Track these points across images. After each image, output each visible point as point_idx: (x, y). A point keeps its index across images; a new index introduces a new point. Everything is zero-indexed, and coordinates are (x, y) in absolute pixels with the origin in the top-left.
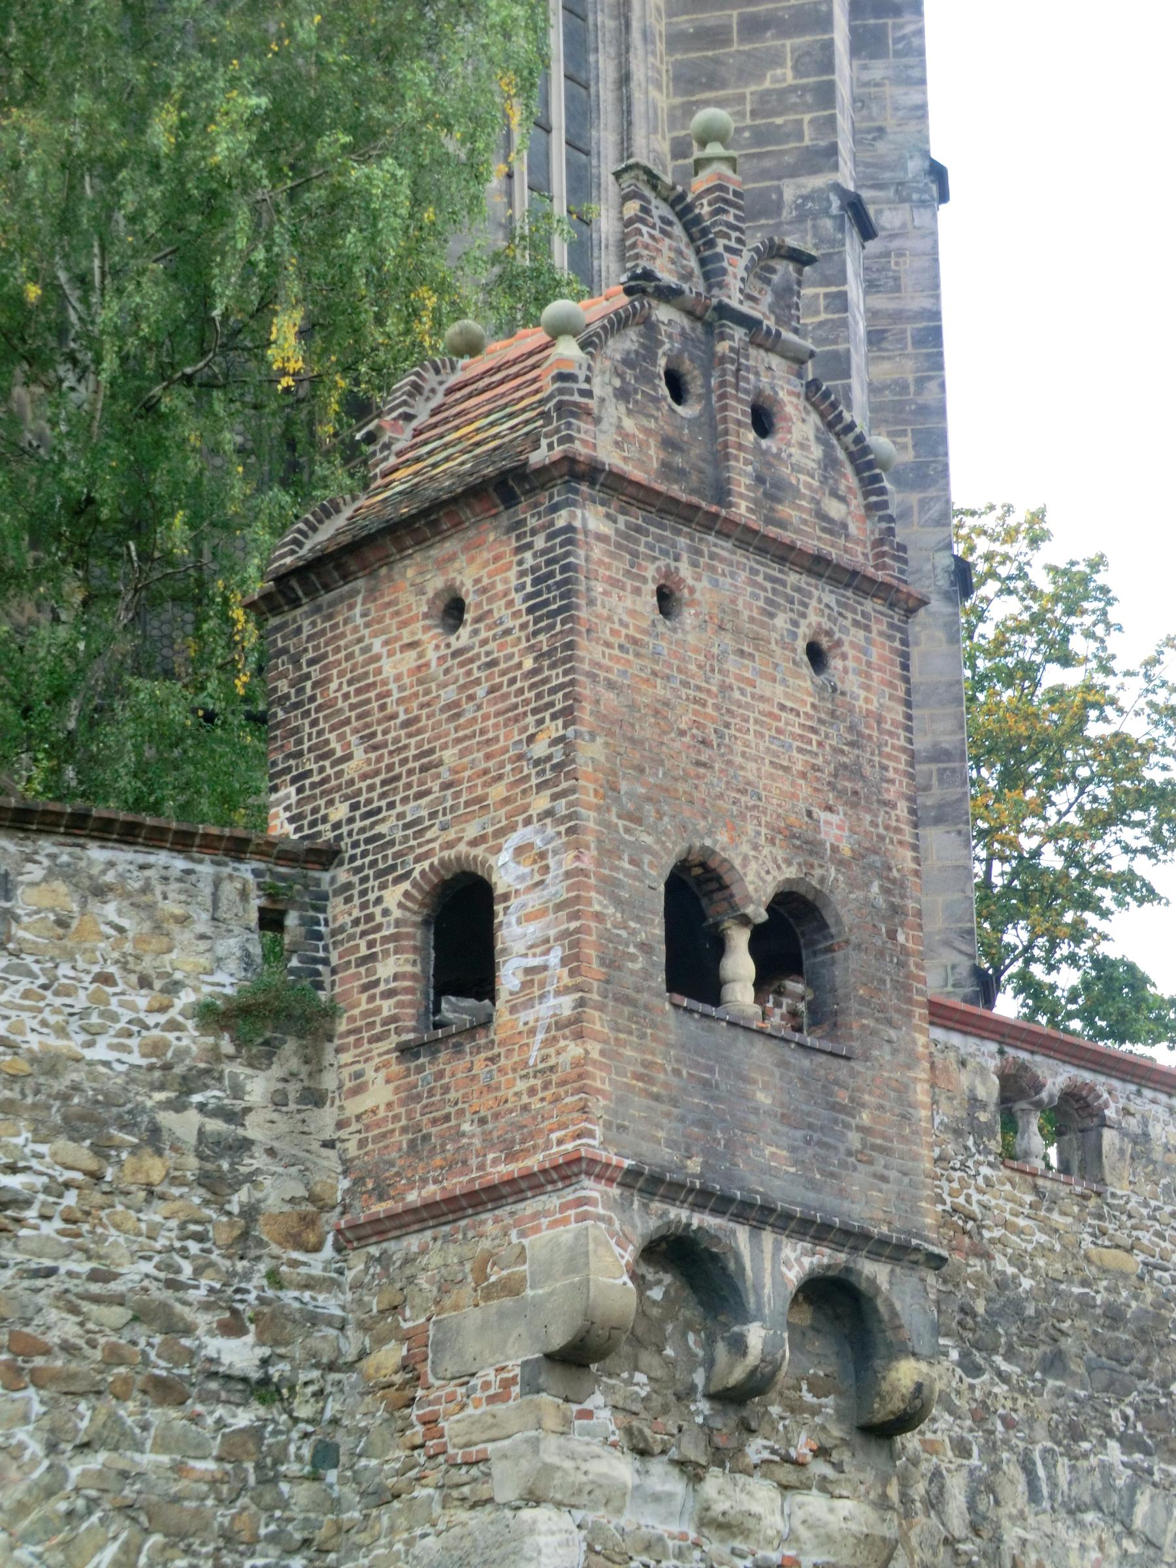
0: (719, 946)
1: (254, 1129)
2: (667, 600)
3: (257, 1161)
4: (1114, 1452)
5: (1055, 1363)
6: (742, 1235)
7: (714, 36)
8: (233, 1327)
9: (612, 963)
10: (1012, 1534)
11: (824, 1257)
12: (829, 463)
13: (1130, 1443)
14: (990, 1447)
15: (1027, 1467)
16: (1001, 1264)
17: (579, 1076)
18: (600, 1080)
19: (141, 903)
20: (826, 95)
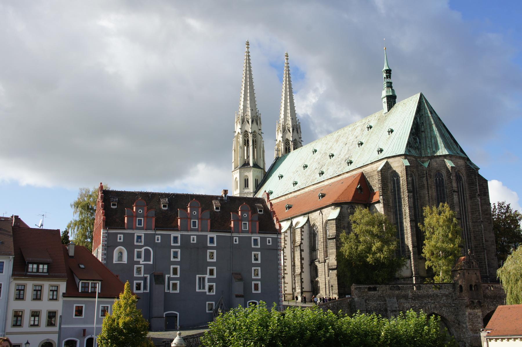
0: (472, 287)
1: (453, 295)
2: (469, 273)
3: (454, 297)
4: (495, 302)
5: (491, 299)
6: (474, 300)
7: (473, 212)
8: (453, 304)
9: (467, 290)
10: (489, 307)
11: (478, 300)
12: (476, 264)
13: (496, 302)
14: (488, 303)
15: (490, 304)
16: (488, 295)
17: (466, 295)
18: (467, 295)
19: (448, 287)
20: (480, 215)
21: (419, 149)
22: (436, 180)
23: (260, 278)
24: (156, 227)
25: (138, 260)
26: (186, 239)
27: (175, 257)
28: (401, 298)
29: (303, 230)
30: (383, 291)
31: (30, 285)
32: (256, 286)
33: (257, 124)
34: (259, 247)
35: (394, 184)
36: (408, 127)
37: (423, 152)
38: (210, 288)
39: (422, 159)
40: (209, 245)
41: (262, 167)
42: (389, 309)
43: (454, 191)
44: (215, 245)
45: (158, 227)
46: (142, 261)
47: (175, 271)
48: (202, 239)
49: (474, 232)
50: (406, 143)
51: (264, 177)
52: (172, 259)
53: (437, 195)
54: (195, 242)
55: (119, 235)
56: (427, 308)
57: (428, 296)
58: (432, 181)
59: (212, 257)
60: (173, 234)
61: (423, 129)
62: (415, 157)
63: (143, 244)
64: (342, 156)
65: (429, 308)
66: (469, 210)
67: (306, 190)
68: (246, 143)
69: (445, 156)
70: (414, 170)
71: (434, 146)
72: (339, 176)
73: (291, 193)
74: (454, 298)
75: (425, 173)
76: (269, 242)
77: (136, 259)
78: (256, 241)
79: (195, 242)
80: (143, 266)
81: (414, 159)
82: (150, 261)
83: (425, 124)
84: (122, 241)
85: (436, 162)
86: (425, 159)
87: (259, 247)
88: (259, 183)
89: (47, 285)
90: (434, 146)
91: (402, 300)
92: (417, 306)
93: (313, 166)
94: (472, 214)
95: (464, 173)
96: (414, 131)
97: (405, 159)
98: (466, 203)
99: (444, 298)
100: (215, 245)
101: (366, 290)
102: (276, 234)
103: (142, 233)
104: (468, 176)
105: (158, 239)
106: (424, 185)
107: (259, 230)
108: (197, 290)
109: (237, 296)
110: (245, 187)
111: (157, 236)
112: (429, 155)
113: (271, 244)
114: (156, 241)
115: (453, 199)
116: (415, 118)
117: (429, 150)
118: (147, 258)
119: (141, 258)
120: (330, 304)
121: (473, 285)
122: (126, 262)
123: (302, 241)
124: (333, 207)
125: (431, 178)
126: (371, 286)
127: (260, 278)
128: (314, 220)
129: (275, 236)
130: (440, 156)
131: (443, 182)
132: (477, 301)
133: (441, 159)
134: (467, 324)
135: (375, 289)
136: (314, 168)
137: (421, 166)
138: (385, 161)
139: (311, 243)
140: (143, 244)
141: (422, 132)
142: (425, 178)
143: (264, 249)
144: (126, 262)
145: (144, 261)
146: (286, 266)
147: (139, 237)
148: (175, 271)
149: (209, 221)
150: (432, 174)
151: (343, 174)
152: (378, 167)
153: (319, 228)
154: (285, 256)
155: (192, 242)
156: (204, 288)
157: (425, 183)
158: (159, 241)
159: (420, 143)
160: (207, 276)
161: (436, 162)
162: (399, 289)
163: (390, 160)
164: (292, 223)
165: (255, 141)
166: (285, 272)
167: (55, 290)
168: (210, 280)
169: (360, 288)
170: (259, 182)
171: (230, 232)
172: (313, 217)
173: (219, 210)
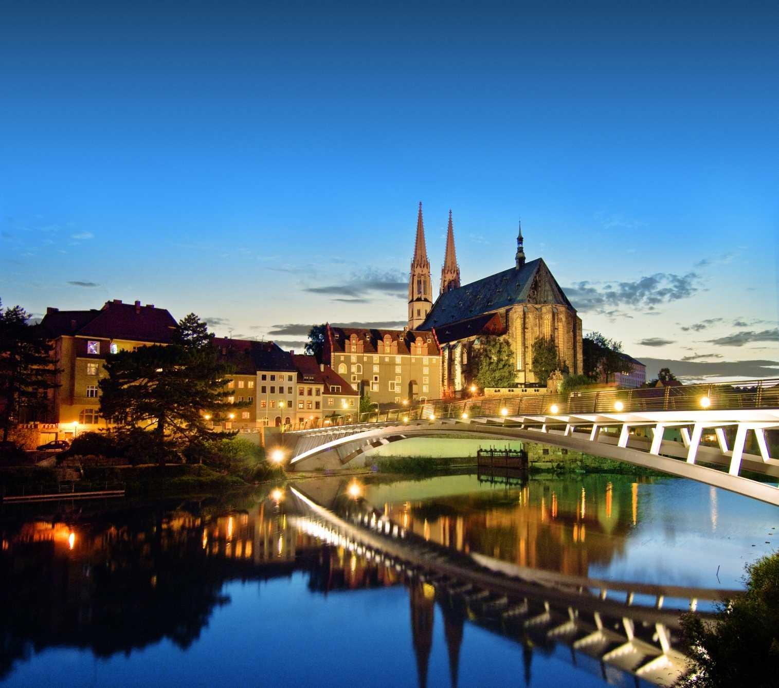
24: (364, 351)
26: (382, 359)
31: (306, 387)
33: (427, 268)
45: (366, 350)
47: (376, 378)
48: (392, 359)
61: (540, 285)
82: (360, 372)
89: (314, 387)
96: (533, 286)
105: (365, 359)
108: (390, 390)
118: (359, 370)
143: (431, 365)
148: (376, 378)
156: (394, 389)
157: (538, 323)
159: (537, 294)
160: (395, 382)
167: (318, 391)
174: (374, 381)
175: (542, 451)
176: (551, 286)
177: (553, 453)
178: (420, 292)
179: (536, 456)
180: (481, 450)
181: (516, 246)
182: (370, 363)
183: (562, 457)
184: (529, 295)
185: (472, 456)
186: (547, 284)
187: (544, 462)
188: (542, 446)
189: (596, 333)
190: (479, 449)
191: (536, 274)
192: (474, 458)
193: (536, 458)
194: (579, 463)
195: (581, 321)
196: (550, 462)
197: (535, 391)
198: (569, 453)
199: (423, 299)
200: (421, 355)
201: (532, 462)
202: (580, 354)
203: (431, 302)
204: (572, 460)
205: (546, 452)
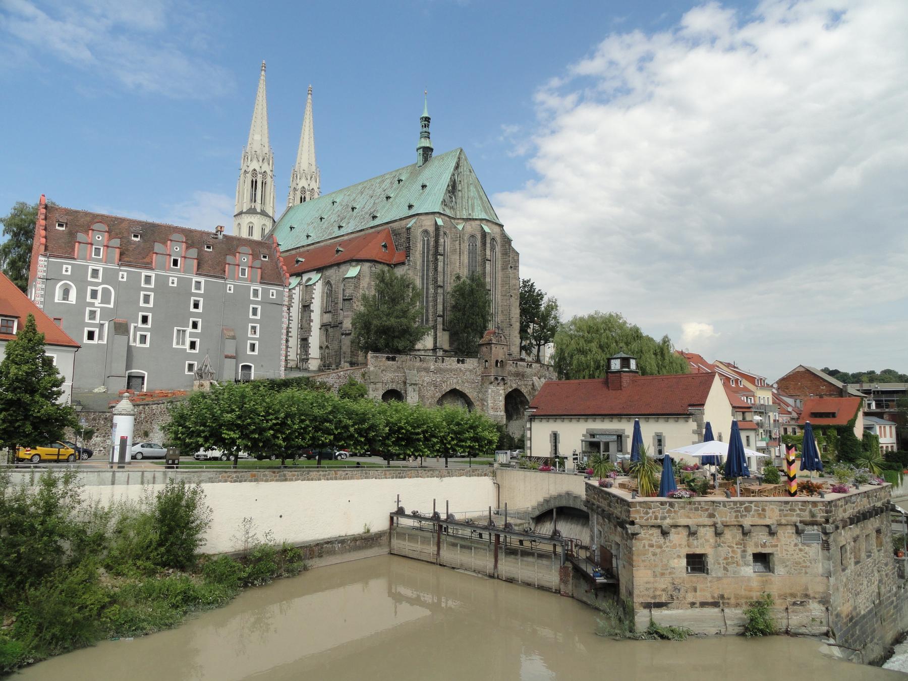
21: (453, 209)
22: (469, 245)
23: (258, 336)
25: (93, 301)
27: (146, 300)
28: (422, 371)
29: (314, 287)
30: (403, 361)
32: (253, 347)
34: (260, 299)
35: (424, 244)
36: (444, 183)
37: (458, 212)
38: (193, 345)
39: (456, 221)
40: (193, 291)
41: (271, 215)
42: (408, 381)
43: (488, 260)
44: (202, 292)
46: (97, 302)
47: (145, 320)
48: (184, 283)
49: (502, 306)
50: (441, 200)
51: (273, 226)
52: (142, 304)
53: (469, 262)
54: (175, 285)
55: (65, 266)
56: (449, 383)
57: (451, 370)
58: (465, 246)
59: (196, 306)
60: (144, 273)
61: (460, 188)
62: (449, 217)
63: (100, 281)
64: (367, 209)
65: (450, 383)
66: (500, 282)
67: (322, 244)
68: (254, 184)
69: (481, 220)
70: (448, 232)
71: (470, 209)
72: (361, 230)
73: (303, 246)
74: (478, 374)
75: (458, 236)
76: (273, 295)
77: (89, 299)
78: (256, 292)
79: (175, 285)
80: (99, 309)
81: (448, 219)
83: (462, 183)
84: (69, 273)
85: (471, 225)
86: (460, 221)
87: (260, 299)
88: (265, 233)
90: (470, 209)
91: (423, 373)
92: (438, 380)
93: (331, 217)
94: (502, 287)
95: (499, 241)
97: (438, 217)
98: (497, 274)
99: (468, 373)
100: (202, 292)
101: (384, 359)
102: (282, 285)
103: (100, 268)
104: (503, 246)
106: (456, 249)
107: (262, 278)
108: (174, 346)
109: (227, 357)
110: (249, 236)
111: (121, 273)
112: (465, 217)
113: (274, 297)
114: (120, 279)
115: (485, 268)
116: (453, 175)
117: (464, 212)
118: (106, 299)
119: (96, 299)
120: (342, 373)
121: (500, 361)
122: (74, 303)
123: (313, 301)
124: (354, 264)
125: (464, 242)
126: (390, 356)
127: (258, 336)
128: (329, 278)
129: (281, 289)
130: (476, 219)
131: (476, 249)
132: (501, 378)
133: (478, 222)
134: (489, 402)
135: (393, 359)
136: (332, 220)
137: (455, 227)
138: (417, 217)
139: (323, 304)
140: (100, 281)
141: (459, 191)
142: (458, 242)
143: (265, 302)
144: (74, 303)
145: (101, 303)
146: (291, 328)
147: (95, 273)
148: (145, 320)
149: (196, 261)
150: (465, 238)
151: (367, 229)
152: (408, 224)
153: (334, 286)
154: (291, 316)
155: (170, 285)
156: (183, 343)
157: (458, 247)
158: (125, 280)
161: (471, 225)
162: (421, 361)
163: (421, 217)
164: (302, 279)
165: (265, 184)
166: (290, 334)
168: (191, 335)
169: (377, 357)
170: (267, 231)
171: (224, 278)
172: (327, 274)
173: (211, 250)
174: (140, 325)
175: (684, 562)
176: (478, 192)
177: (725, 569)
178: (253, 199)
179: (663, 583)
180: (400, 512)
181: (418, 127)
182: (133, 286)
183: (755, 584)
184: (444, 200)
185: (375, 529)
186: (472, 188)
187: (693, 604)
188: (684, 542)
189: (528, 281)
190: (395, 509)
191: (455, 170)
192: (379, 535)
193: (664, 590)
194: (816, 609)
195: (518, 254)
196: (715, 604)
197: (458, 361)
198: (780, 570)
199: (259, 210)
200: (245, 280)
201: (648, 606)
202: (516, 308)
203: (270, 217)
204: (793, 595)
205: (696, 563)
